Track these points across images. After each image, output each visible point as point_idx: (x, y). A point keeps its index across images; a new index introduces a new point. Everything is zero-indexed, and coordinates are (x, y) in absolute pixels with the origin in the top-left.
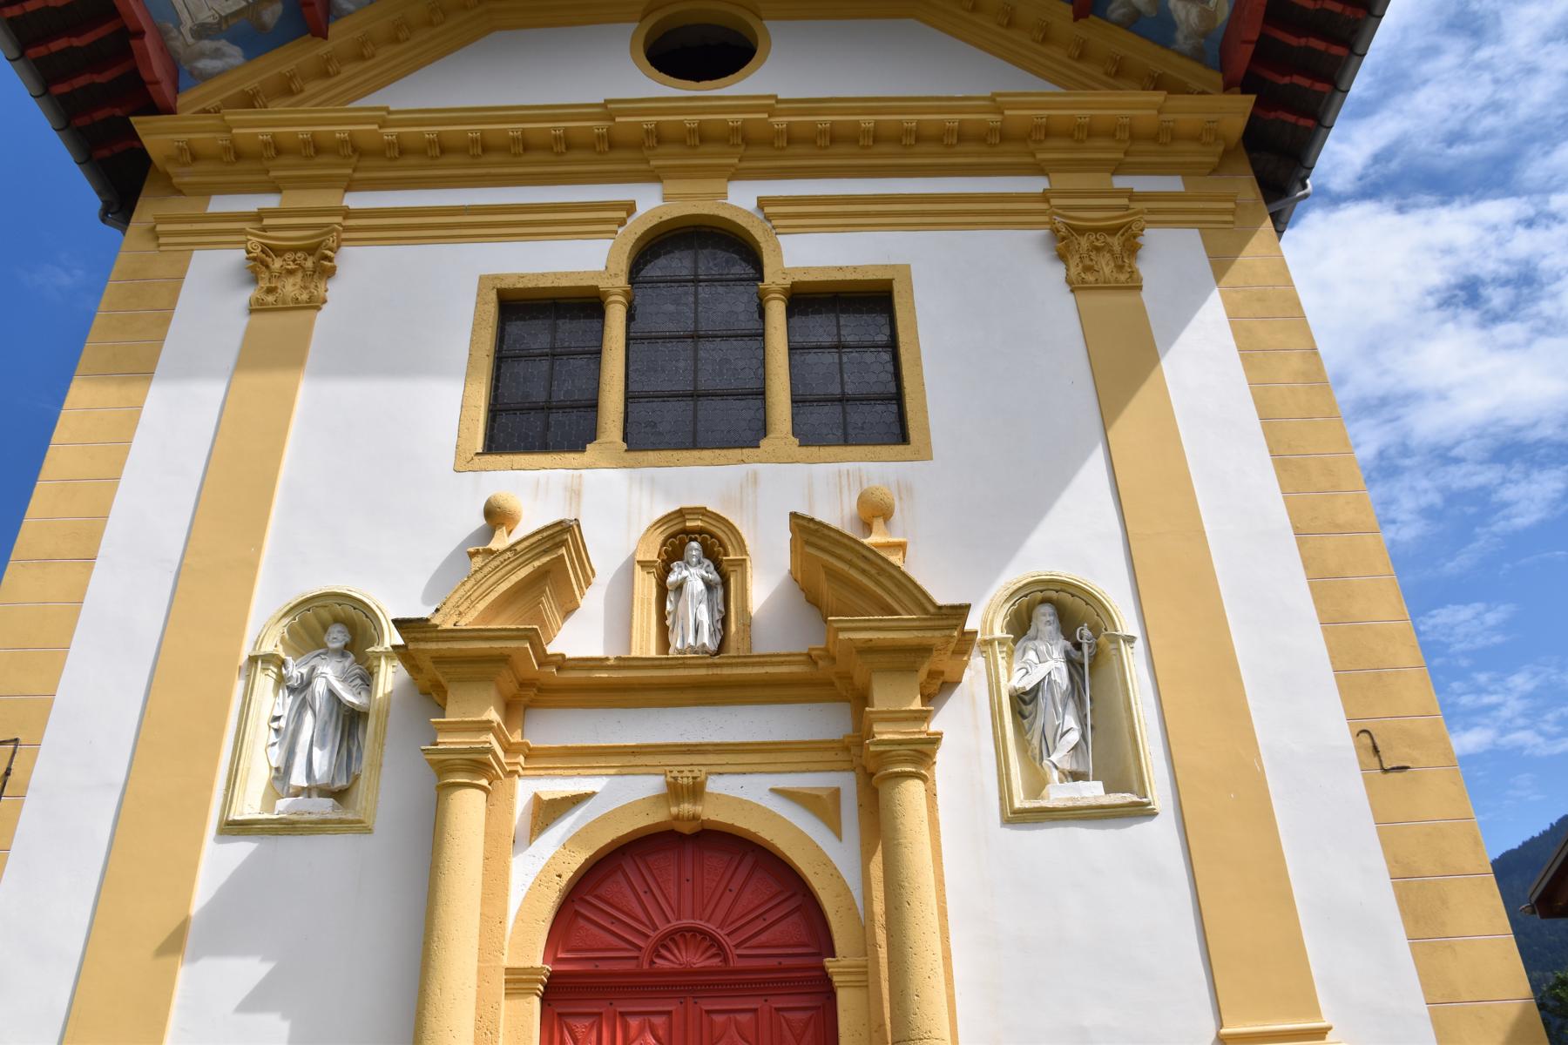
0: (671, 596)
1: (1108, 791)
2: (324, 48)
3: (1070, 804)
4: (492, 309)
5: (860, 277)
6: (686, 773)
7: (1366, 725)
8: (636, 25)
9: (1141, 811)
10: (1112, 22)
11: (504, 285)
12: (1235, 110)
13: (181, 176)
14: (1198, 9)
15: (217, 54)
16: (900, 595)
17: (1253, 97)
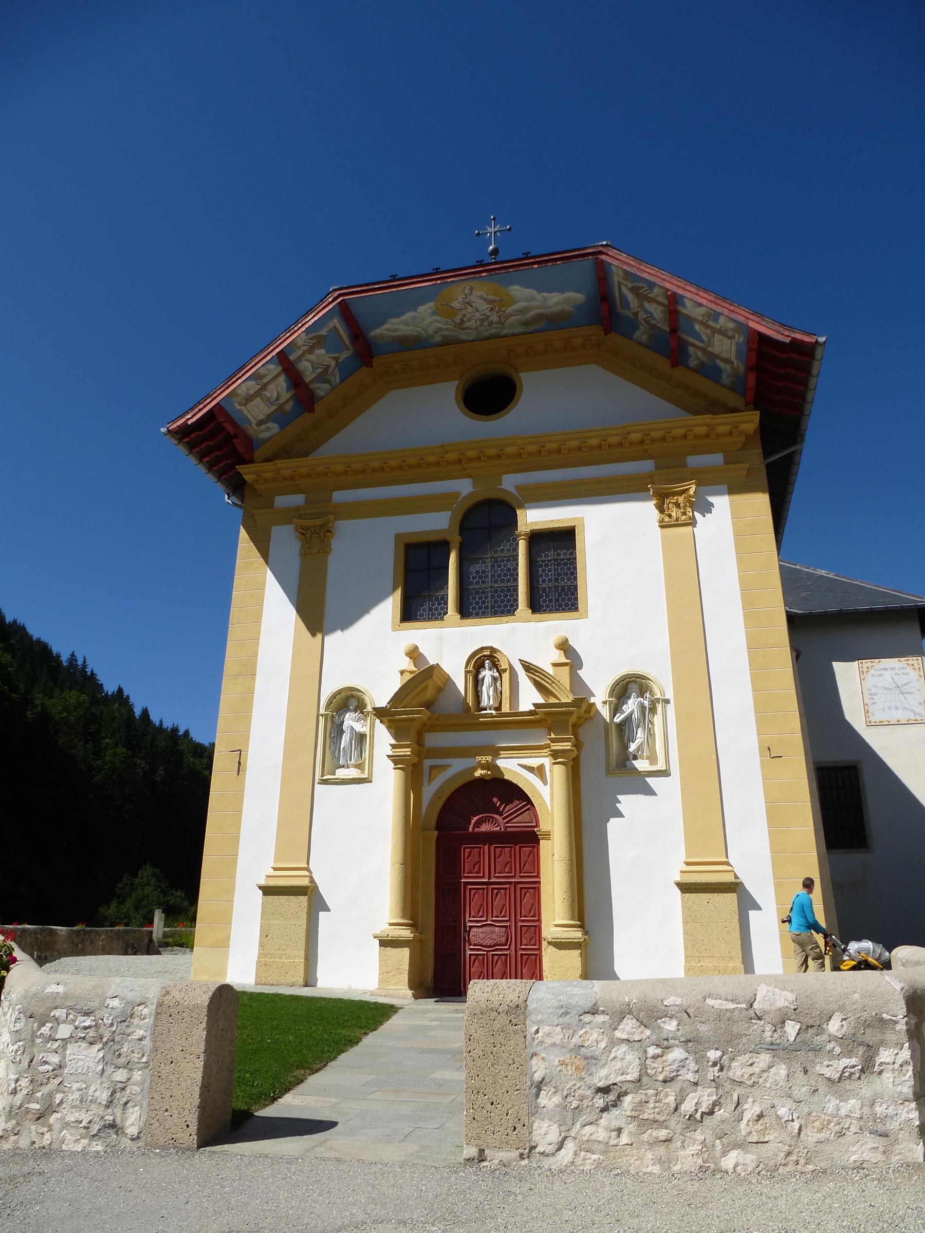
1: (651, 764)
5: (560, 525)
6: (484, 759)
8: (458, 381)
15: (268, 429)
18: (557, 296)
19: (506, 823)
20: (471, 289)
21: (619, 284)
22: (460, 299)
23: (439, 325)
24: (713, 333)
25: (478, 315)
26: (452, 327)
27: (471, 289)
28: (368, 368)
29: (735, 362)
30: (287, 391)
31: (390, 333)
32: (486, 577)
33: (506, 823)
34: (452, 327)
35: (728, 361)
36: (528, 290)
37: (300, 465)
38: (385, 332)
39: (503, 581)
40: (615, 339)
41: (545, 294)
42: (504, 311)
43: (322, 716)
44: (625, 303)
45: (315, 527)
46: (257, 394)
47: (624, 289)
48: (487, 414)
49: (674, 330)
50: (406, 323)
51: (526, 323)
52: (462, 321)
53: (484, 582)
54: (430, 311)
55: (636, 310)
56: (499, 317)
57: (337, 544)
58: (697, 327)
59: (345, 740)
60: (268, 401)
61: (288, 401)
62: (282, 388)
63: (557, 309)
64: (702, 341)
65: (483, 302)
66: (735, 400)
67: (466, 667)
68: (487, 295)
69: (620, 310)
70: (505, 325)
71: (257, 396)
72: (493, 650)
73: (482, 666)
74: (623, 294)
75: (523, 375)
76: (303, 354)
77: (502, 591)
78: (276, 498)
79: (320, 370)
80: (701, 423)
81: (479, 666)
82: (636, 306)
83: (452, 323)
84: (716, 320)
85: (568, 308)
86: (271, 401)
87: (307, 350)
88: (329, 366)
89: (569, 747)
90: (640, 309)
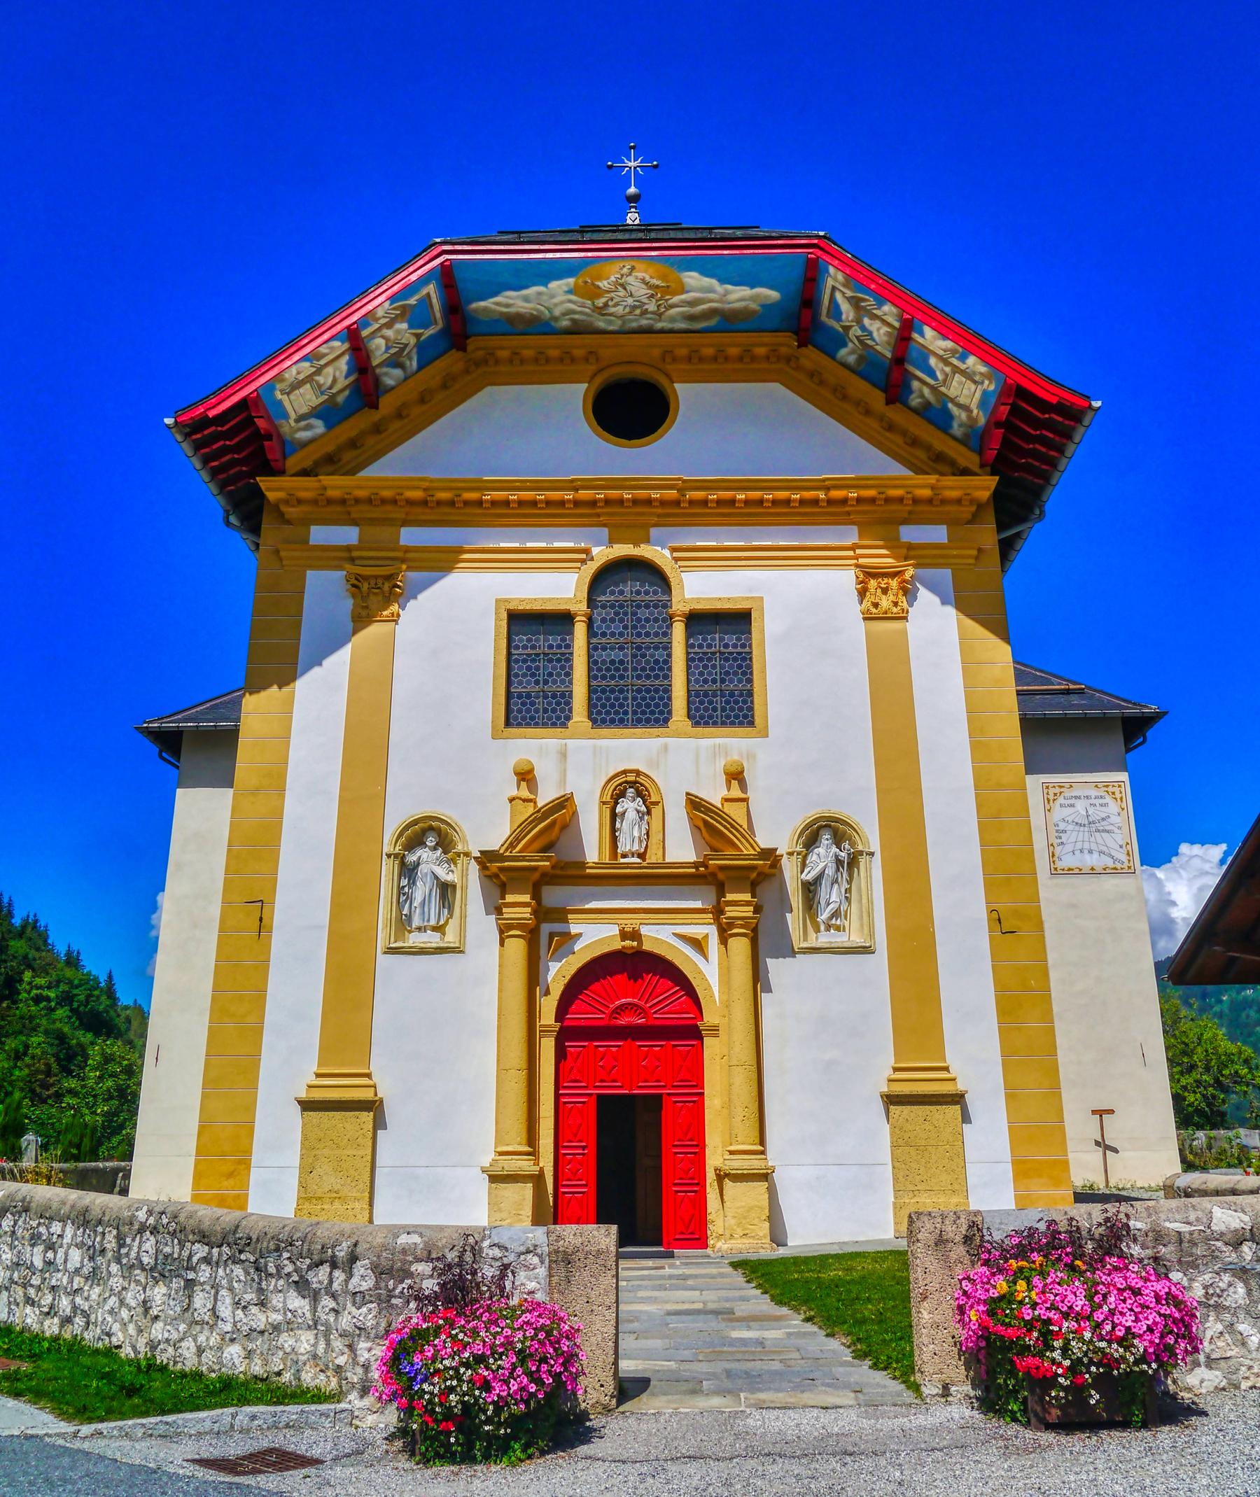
0: (618, 820)
2: (375, 416)
3: (828, 946)
4: (504, 623)
7: (995, 906)
8: (586, 385)
9: (866, 950)
11: (511, 606)
12: (984, 486)
13: (291, 512)
16: (742, 840)
17: (997, 478)
19: (655, 1013)
20: (633, 268)
21: (834, 288)
22: (613, 279)
24: (954, 373)
26: (587, 310)
27: (633, 268)
29: (975, 411)
30: (346, 377)
31: (498, 308)
32: (626, 669)
33: (655, 1013)
38: (493, 307)
40: (811, 357)
41: (729, 287)
42: (667, 300)
43: (389, 856)
44: (835, 311)
45: (376, 577)
46: (309, 379)
47: (838, 296)
49: (900, 359)
50: (526, 299)
51: (691, 318)
52: (606, 305)
53: (622, 677)
54: (566, 289)
58: (933, 361)
59: (421, 891)
60: (319, 389)
62: (341, 372)
64: (935, 378)
65: (644, 286)
66: (969, 459)
67: (602, 795)
68: (651, 277)
69: (824, 318)
71: (305, 383)
72: (638, 773)
73: (622, 794)
75: (678, 386)
76: (379, 329)
78: (313, 528)
79: (393, 351)
80: (923, 485)
81: (619, 795)
85: (754, 306)
86: (323, 389)
87: (385, 324)
88: (406, 345)
89: (751, 914)
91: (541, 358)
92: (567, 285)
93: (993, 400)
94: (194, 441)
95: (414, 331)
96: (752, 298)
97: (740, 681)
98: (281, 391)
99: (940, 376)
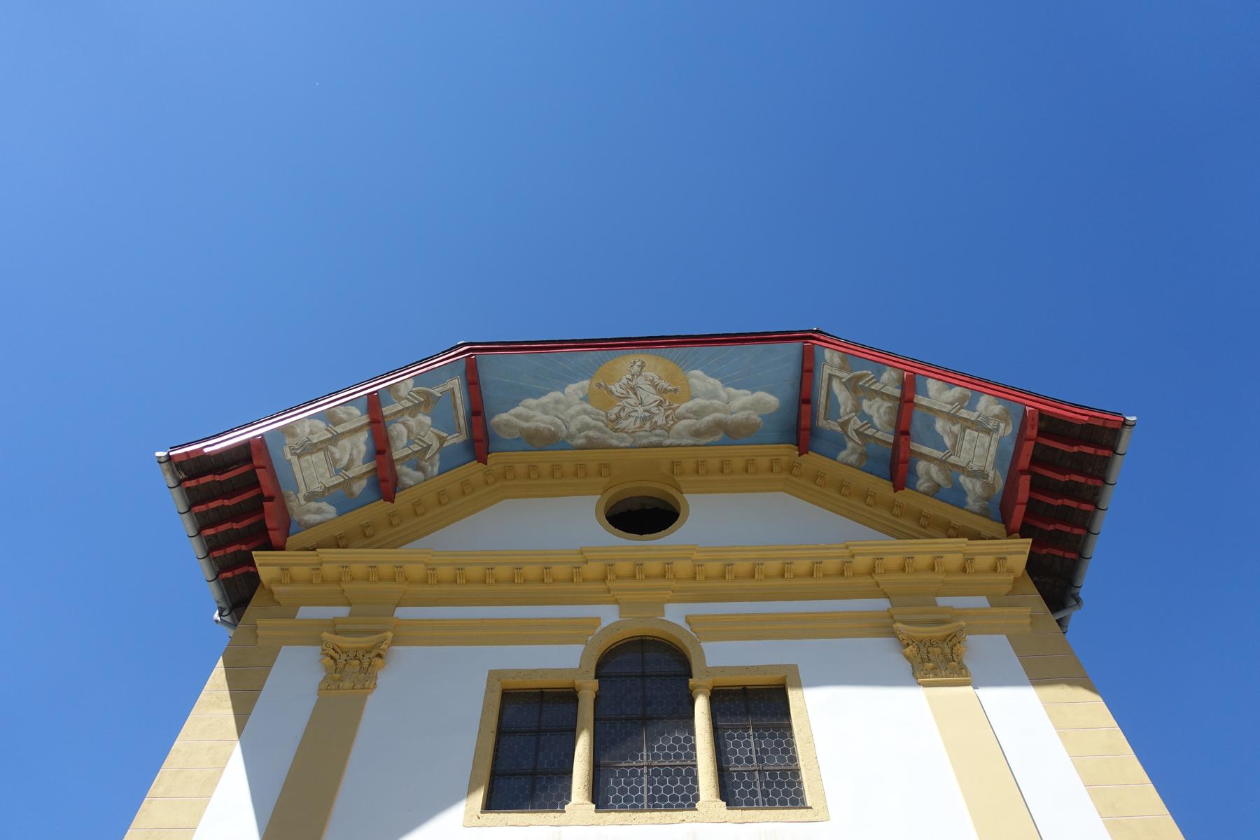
8: (600, 496)
10: (921, 492)
12: (1018, 551)
14: (981, 482)
15: (319, 511)
17: (1030, 540)
18: (746, 395)
20: (642, 366)
21: (831, 377)
22: (625, 381)
23: (587, 419)
25: (640, 409)
26: (602, 424)
27: (642, 366)
28: (481, 464)
29: (991, 474)
34: (602, 424)
35: (980, 474)
36: (712, 380)
37: (358, 558)
38: (515, 420)
39: (667, 757)
40: (812, 460)
41: (731, 390)
47: (836, 386)
48: (641, 534)
49: (903, 431)
51: (697, 433)
52: (618, 417)
54: (582, 396)
55: (846, 418)
56: (667, 417)
57: (387, 678)
58: (939, 425)
61: (359, 477)
62: (359, 452)
63: (740, 416)
64: (940, 445)
65: (653, 390)
68: (660, 378)
69: (822, 422)
70: (671, 433)
71: (319, 450)
74: (833, 392)
77: (667, 773)
79: (417, 448)
82: (848, 410)
83: (606, 421)
84: (972, 407)
85: (755, 417)
87: (408, 408)
88: (429, 446)
90: (854, 414)
91: (555, 471)
92: (582, 389)
93: (1011, 448)
94: (188, 490)
95: (438, 432)
96: (755, 405)
97: (781, 760)
98: (292, 449)
99: (948, 442)
